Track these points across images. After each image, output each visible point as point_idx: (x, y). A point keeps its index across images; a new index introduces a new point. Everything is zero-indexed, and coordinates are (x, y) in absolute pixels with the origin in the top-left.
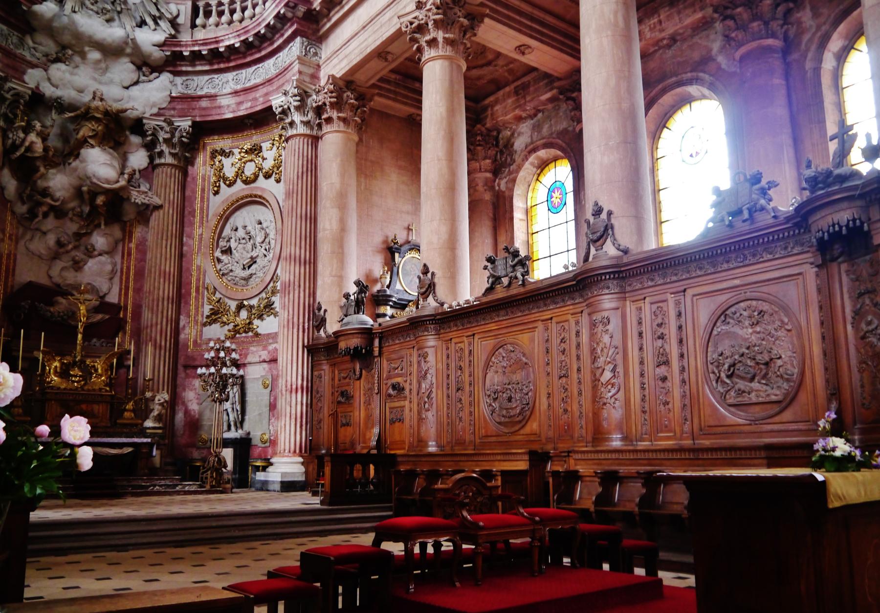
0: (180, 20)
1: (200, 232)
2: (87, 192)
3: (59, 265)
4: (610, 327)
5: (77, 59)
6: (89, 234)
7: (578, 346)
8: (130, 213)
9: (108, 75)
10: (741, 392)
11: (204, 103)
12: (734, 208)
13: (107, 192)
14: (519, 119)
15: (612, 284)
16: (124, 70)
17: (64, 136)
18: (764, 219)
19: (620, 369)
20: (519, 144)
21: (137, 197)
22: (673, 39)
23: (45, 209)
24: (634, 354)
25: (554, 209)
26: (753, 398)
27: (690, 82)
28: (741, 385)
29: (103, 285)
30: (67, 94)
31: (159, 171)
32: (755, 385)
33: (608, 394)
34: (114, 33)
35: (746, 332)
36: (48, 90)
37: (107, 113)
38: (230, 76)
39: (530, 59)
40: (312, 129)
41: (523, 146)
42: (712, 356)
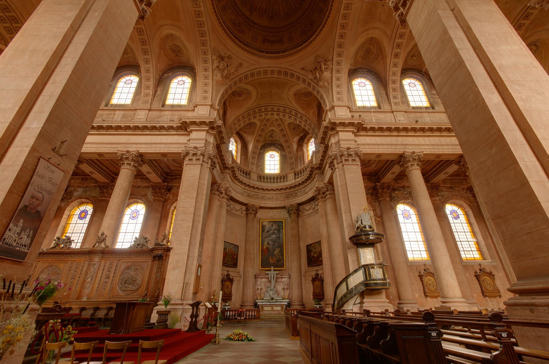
4: (95, 267)
7: (82, 270)
10: (126, 287)
12: (139, 243)
14: (79, 187)
15: (100, 255)
18: (145, 248)
19: (94, 279)
20: (76, 194)
22: (139, 187)
24: (99, 275)
25: (80, 218)
26: (129, 289)
27: (139, 199)
28: (127, 285)
32: (130, 286)
33: (87, 285)
35: (132, 273)
39: (93, 176)
41: (77, 195)
42: (122, 277)
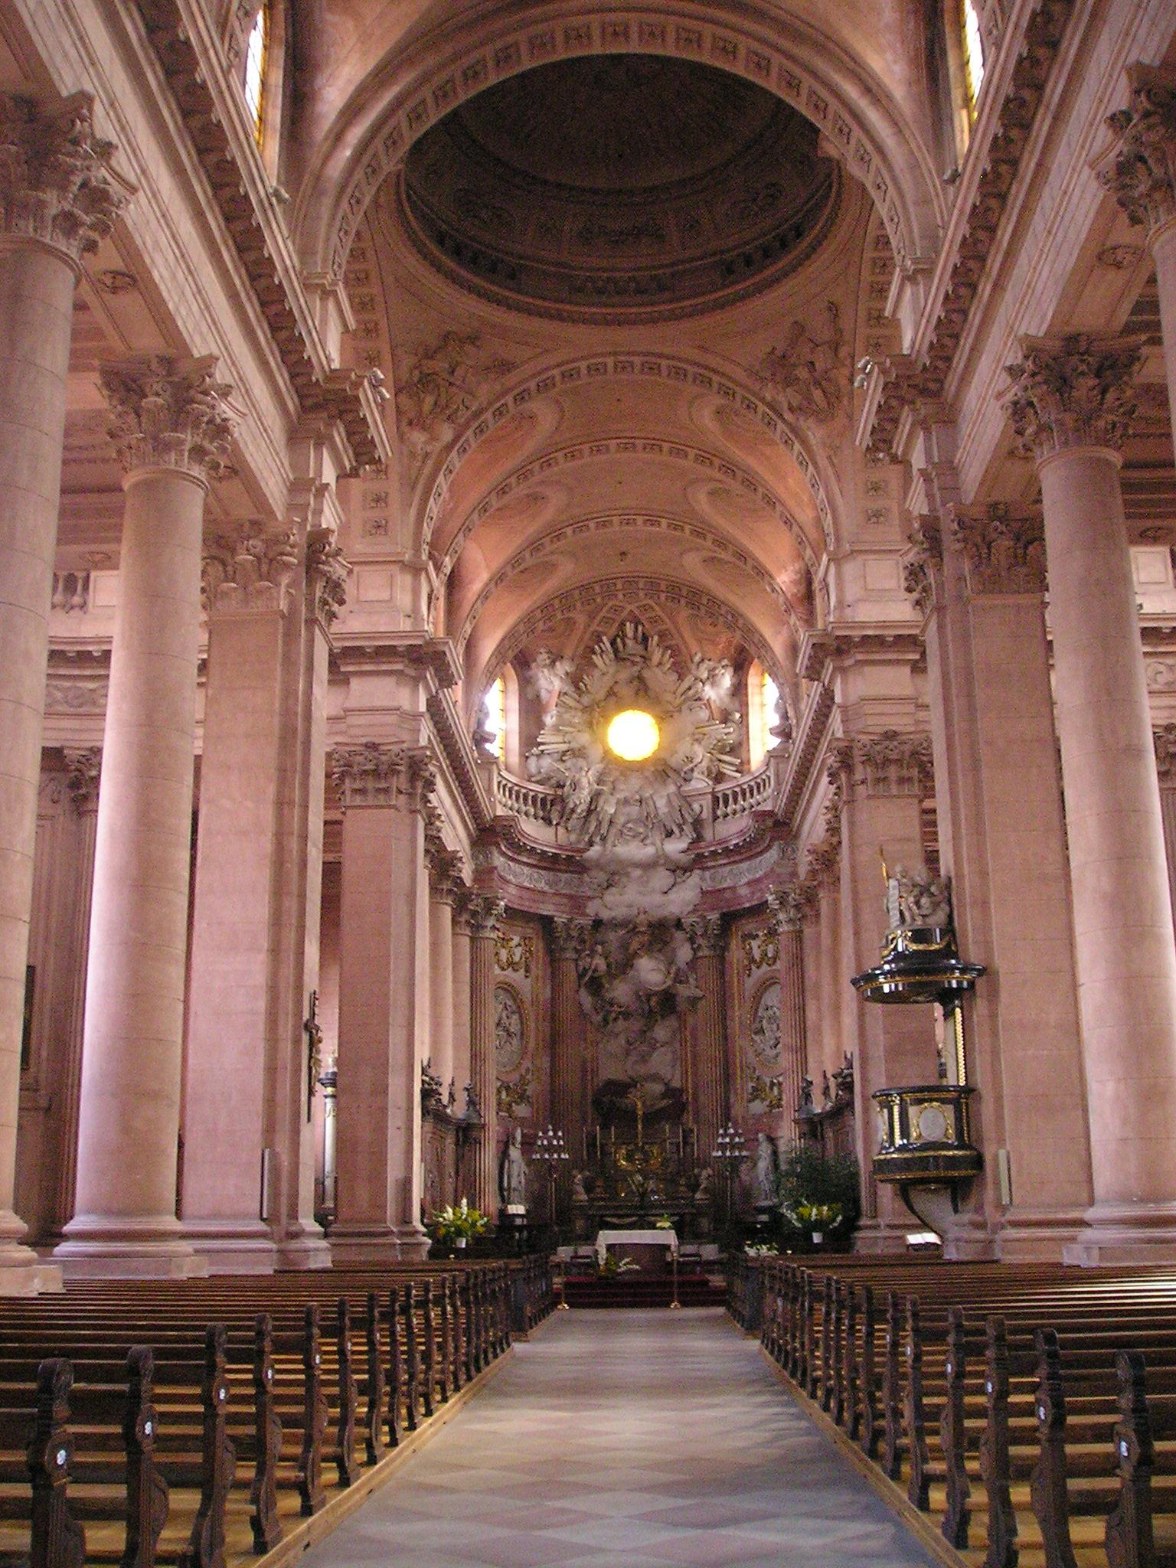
0: (704, 815)
1: (739, 1013)
2: (644, 995)
3: (632, 1059)
5: (624, 879)
6: (651, 1028)
8: (682, 1006)
9: (651, 885)
11: (728, 895)
13: (656, 993)
16: (661, 878)
17: (624, 946)
21: (684, 991)
23: (613, 1015)
29: (666, 1072)
30: (620, 913)
31: (700, 961)
34: (650, 850)
36: (605, 915)
37: (650, 925)
38: (744, 865)
40: (794, 925)
